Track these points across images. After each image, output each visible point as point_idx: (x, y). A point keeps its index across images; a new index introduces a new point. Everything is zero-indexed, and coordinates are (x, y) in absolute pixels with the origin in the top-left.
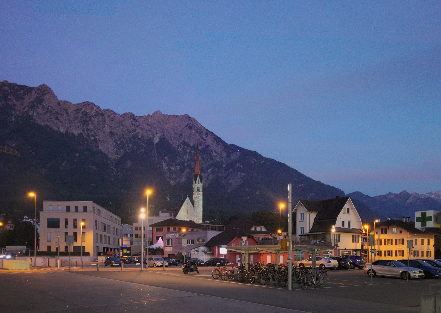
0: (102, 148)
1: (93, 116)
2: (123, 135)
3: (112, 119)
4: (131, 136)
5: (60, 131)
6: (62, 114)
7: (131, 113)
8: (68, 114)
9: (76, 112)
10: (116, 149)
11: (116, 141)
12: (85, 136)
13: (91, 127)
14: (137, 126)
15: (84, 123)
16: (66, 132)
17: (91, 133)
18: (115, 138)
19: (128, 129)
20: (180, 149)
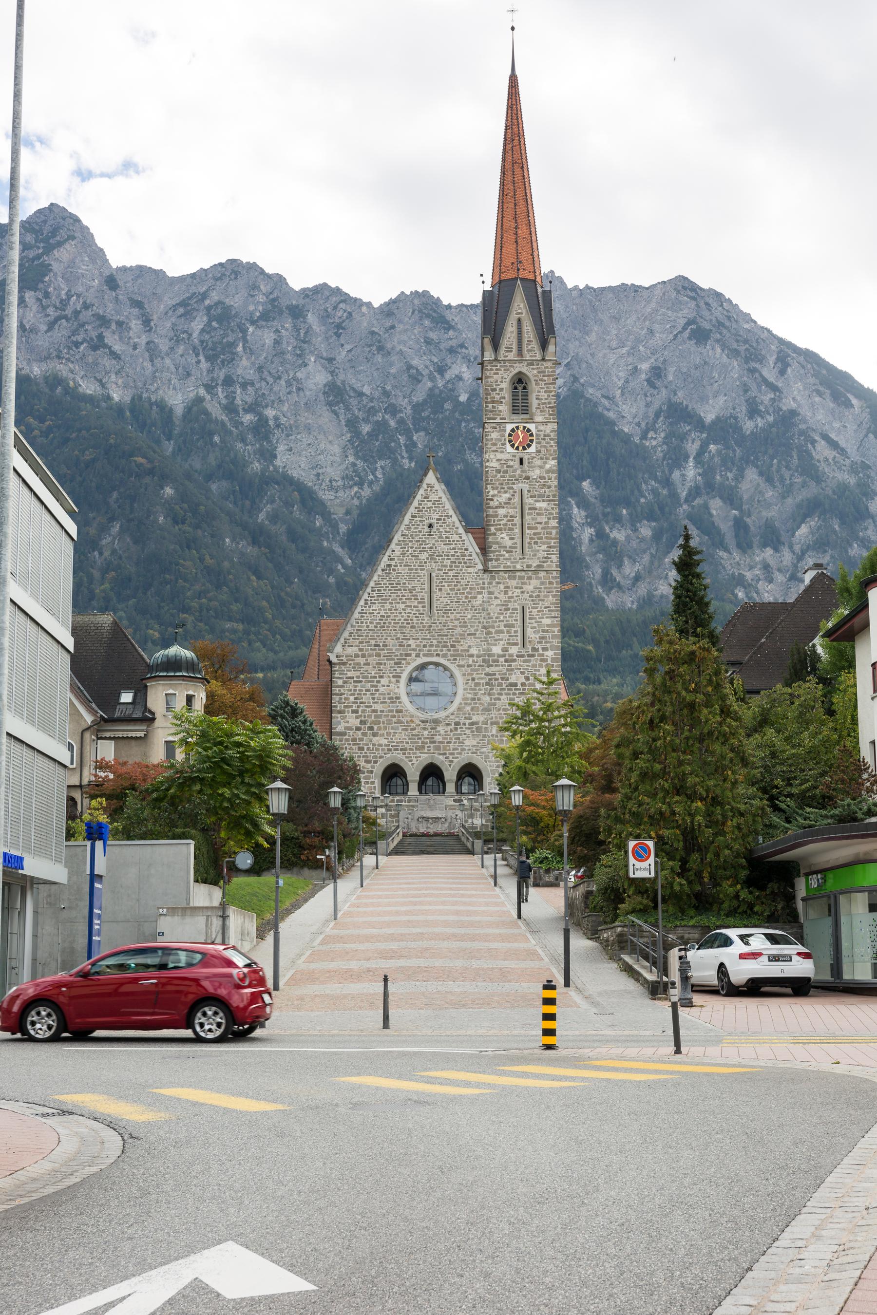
1: (253, 323)
2: (386, 394)
3: (339, 326)
6: (120, 324)
7: (426, 294)
8: (147, 322)
9: (181, 310)
10: (351, 459)
11: (352, 424)
12: (215, 409)
13: (244, 368)
14: (452, 351)
15: (218, 353)
16: (136, 400)
17: (241, 397)
18: (348, 409)
19: (410, 367)
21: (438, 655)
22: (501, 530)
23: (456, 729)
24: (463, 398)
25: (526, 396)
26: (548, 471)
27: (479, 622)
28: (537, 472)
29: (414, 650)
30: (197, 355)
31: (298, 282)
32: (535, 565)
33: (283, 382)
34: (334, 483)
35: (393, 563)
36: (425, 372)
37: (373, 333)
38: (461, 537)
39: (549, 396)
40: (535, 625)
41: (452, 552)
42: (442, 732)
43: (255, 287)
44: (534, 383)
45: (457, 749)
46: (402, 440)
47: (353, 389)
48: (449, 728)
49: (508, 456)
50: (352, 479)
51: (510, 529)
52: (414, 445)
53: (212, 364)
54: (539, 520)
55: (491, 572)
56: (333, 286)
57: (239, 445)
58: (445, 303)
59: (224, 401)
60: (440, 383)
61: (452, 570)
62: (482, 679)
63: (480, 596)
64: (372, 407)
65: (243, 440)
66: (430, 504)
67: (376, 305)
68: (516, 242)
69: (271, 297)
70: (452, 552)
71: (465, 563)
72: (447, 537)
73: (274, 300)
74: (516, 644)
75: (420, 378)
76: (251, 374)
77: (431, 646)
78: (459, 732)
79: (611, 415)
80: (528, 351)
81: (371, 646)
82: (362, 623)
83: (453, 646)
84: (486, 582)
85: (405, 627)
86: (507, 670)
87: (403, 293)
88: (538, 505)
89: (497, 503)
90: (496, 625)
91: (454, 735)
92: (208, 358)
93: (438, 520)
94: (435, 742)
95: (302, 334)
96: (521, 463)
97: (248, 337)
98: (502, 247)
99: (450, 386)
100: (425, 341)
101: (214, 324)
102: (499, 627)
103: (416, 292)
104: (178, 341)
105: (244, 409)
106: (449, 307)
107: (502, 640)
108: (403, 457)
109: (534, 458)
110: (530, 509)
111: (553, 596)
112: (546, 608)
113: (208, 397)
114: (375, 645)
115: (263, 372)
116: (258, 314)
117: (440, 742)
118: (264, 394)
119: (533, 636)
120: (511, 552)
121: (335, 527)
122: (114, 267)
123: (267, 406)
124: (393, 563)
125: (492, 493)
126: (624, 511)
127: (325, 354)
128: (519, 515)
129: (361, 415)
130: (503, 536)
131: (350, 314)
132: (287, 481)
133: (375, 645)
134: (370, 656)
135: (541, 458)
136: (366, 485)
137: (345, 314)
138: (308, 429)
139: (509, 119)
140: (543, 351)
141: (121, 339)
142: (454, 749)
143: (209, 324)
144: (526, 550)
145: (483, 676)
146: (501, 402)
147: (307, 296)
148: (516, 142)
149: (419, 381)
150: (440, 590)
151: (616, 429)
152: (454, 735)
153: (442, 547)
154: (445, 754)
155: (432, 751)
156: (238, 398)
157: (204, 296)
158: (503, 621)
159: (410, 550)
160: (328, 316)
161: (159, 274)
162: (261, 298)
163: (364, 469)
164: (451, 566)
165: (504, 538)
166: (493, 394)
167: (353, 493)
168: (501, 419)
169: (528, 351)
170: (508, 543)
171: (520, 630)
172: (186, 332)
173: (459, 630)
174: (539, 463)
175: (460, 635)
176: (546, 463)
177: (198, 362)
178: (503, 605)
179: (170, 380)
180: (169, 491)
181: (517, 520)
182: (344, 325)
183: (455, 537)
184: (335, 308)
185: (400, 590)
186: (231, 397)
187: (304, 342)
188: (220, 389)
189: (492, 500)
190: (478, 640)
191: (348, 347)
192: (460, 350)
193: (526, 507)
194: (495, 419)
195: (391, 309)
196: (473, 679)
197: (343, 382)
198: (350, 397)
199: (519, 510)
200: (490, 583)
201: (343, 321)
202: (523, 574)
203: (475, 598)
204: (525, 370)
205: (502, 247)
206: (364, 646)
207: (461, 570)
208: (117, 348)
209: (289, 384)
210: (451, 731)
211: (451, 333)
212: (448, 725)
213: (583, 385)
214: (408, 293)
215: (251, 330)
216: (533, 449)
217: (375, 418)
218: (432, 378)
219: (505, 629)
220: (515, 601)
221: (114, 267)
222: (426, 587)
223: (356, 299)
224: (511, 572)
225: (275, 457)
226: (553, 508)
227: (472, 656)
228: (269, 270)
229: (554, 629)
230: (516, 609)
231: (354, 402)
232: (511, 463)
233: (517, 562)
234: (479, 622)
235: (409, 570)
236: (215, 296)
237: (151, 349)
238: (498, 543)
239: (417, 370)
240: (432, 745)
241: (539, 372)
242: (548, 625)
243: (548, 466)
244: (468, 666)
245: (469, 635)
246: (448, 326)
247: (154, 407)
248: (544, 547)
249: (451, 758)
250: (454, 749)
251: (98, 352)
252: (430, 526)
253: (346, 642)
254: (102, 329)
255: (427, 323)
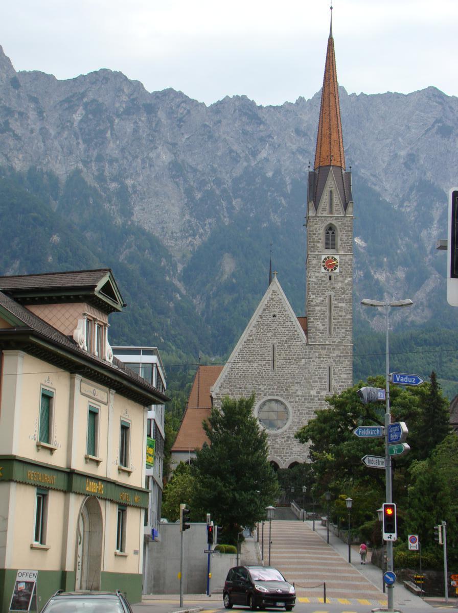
0: (144, 216)
1: (118, 116)
2: (214, 170)
3: (180, 120)
4: (238, 171)
5: (12, 169)
6: (21, 114)
7: (244, 97)
8: (40, 113)
9: (66, 105)
10: (187, 217)
11: (189, 192)
12: (90, 181)
13: (112, 149)
14: (262, 140)
16: (32, 170)
17: (108, 170)
18: (186, 181)
19: (231, 151)
20: (409, 209)
21: (277, 395)
22: (317, 319)
23: (288, 441)
24: (270, 174)
25: (334, 238)
26: (346, 285)
27: (303, 376)
28: (340, 285)
29: (262, 391)
30: (77, 139)
31: (152, 86)
32: (337, 341)
33: (139, 160)
34: (174, 235)
35: (251, 338)
36: (242, 155)
37: (205, 126)
38: (292, 324)
39: (348, 238)
40: (337, 378)
41: (287, 332)
42: (279, 442)
43: (120, 90)
44: (339, 230)
45: (288, 453)
46: (224, 204)
47: (191, 167)
48: (283, 440)
49: (322, 275)
50: (188, 232)
51: (322, 319)
52: (233, 208)
53: (88, 145)
54: (340, 314)
55: (311, 345)
56: (177, 90)
57: (107, 205)
58: (258, 104)
59: (96, 173)
60: (253, 164)
61: (287, 343)
62: (304, 410)
63: (303, 360)
64: (204, 180)
65: (110, 202)
66: (274, 303)
67: (208, 105)
68: (330, 143)
69: (132, 97)
70: (287, 332)
71: (295, 339)
72: (284, 323)
73: (134, 100)
74: (325, 390)
75: (239, 159)
76: (116, 154)
77: (273, 389)
78: (289, 442)
79: (377, 188)
80: (336, 210)
81: (237, 388)
82: (232, 374)
83: (286, 390)
84: (307, 350)
85: (258, 377)
86: (319, 405)
87: (227, 96)
88: (340, 305)
89: (315, 303)
90: (313, 377)
91: (286, 444)
92: (85, 141)
93: (279, 312)
94: (275, 448)
95: (154, 125)
96: (330, 278)
97: (115, 127)
98: (321, 146)
99: (260, 165)
100: (243, 132)
101: (90, 116)
102: (315, 379)
103: (238, 96)
104: (63, 128)
105: (110, 179)
106: (261, 107)
107: (316, 387)
108: (225, 217)
109: (338, 276)
110: (335, 307)
111: (348, 361)
112: (343, 368)
113: (85, 170)
114: (240, 388)
115: (125, 152)
116: (122, 110)
117: (277, 448)
118: (125, 169)
119: (336, 385)
120: (323, 333)
121: (175, 266)
122: (17, 71)
123: (127, 177)
124: (251, 338)
125: (312, 297)
126: (385, 259)
127: (170, 140)
128: (328, 311)
129: (195, 185)
130: (318, 323)
131: (189, 112)
132: (140, 232)
133: (240, 388)
134: (236, 394)
135: (343, 277)
136: (197, 237)
137: (185, 111)
138: (157, 194)
139: (328, 66)
140: (345, 210)
141: (22, 125)
142: (286, 453)
143: (86, 116)
144: (332, 332)
145: (304, 408)
146: (319, 242)
147: (158, 97)
148: (331, 80)
149: (238, 162)
150: (279, 355)
151: (381, 199)
152: (286, 444)
153: (281, 329)
154: (281, 456)
155: (273, 454)
156: (106, 171)
157: (83, 95)
158: (317, 375)
159: (262, 330)
160: (173, 113)
161: (51, 78)
162: (125, 98)
163: (197, 225)
164: (286, 341)
165: (319, 324)
166: (314, 237)
167: (188, 242)
168: (318, 252)
169: (336, 210)
170: (322, 328)
171: (327, 381)
172: (69, 121)
173: (290, 380)
174: (341, 279)
175: (291, 383)
176: (345, 279)
177: (78, 144)
178: (318, 366)
179: (57, 157)
180: (56, 238)
181: (327, 314)
182: (184, 118)
183: (289, 323)
184: (178, 106)
185: (255, 355)
186: (101, 170)
187: (155, 131)
188: (93, 164)
189: (312, 301)
190: (302, 387)
191: (186, 137)
192: (267, 139)
193: (333, 306)
194: (315, 252)
195: (219, 107)
196: (299, 410)
197: (183, 161)
198: (188, 172)
199: (328, 308)
200: (310, 352)
201: (184, 116)
202: (330, 347)
203: (301, 360)
204: (333, 222)
205: (321, 146)
206: (233, 388)
207: (292, 343)
208: (19, 132)
209: (143, 161)
210: (285, 442)
211: (262, 127)
212: (283, 438)
213: (357, 166)
214: (231, 97)
215: (116, 121)
216: (337, 271)
217: (206, 188)
218: (247, 159)
219: (319, 380)
220: (325, 363)
221: (17, 71)
222: (271, 353)
223: (193, 101)
224: (323, 346)
225: (133, 214)
226: (349, 307)
227: (298, 396)
228: (131, 77)
229: (348, 381)
230: (325, 368)
231: (190, 176)
232: (324, 279)
233: (327, 340)
234: (303, 376)
235: (261, 342)
236: (91, 96)
237: (44, 132)
238: (315, 328)
239: (237, 154)
240: (273, 450)
241: (342, 224)
242: (345, 379)
243: (346, 281)
244: (296, 402)
245: (296, 383)
246: (260, 121)
247: (45, 176)
248: (343, 331)
249: (284, 459)
250: (286, 453)
251: (5, 134)
252: (274, 316)
253: (222, 386)
254: (8, 118)
255: (244, 119)
